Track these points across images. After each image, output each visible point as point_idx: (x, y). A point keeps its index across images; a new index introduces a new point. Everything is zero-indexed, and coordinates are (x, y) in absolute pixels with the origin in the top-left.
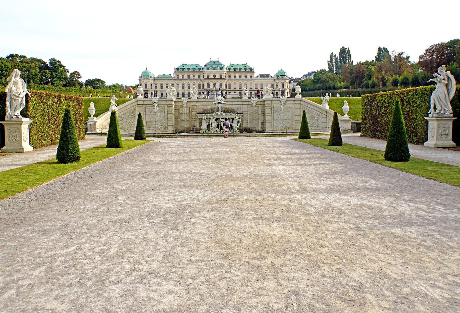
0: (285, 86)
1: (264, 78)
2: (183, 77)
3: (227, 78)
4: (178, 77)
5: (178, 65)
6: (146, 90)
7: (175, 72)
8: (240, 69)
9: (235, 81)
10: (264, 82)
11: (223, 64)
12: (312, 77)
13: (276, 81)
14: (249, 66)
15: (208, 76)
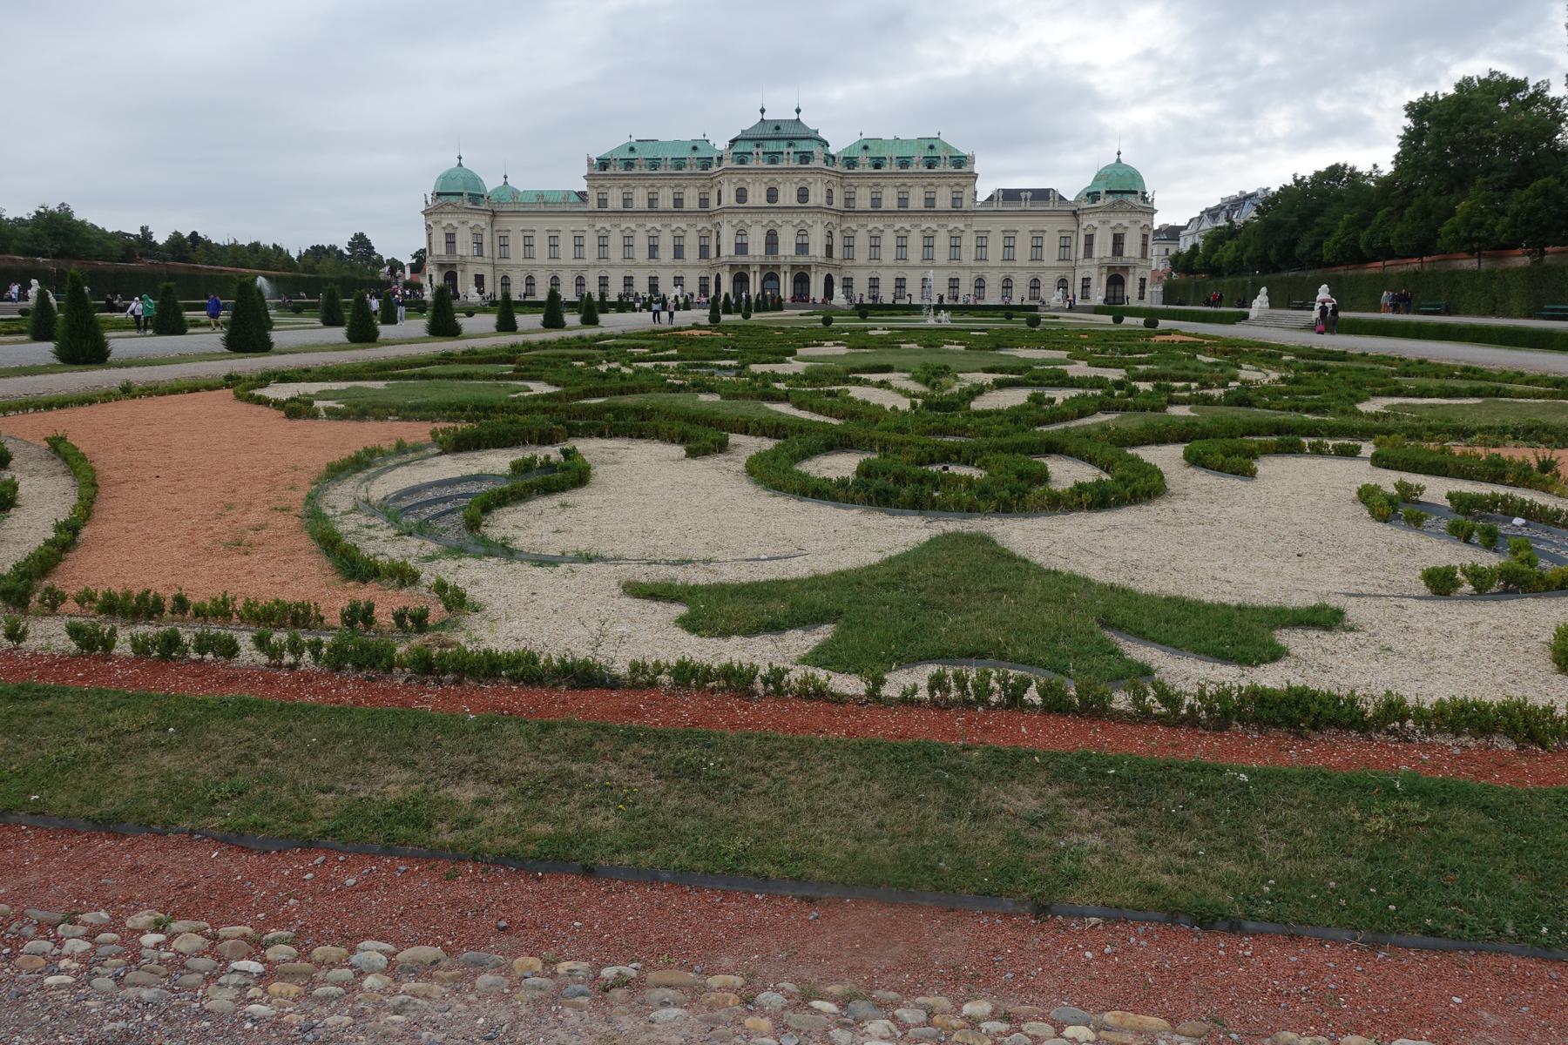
0: (1131, 249)
1: (1023, 206)
2: (627, 201)
3: (838, 203)
4: (602, 202)
5: (609, 143)
6: (446, 260)
7: (589, 177)
8: (904, 162)
9: (875, 224)
10: (1024, 228)
11: (822, 134)
12: (1249, 213)
13: (1086, 221)
14: (947, 147)
15: (741, 195)
